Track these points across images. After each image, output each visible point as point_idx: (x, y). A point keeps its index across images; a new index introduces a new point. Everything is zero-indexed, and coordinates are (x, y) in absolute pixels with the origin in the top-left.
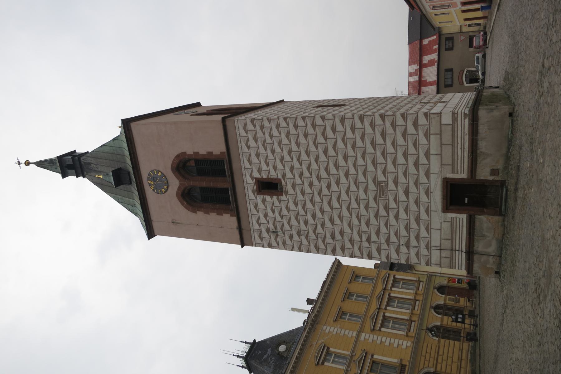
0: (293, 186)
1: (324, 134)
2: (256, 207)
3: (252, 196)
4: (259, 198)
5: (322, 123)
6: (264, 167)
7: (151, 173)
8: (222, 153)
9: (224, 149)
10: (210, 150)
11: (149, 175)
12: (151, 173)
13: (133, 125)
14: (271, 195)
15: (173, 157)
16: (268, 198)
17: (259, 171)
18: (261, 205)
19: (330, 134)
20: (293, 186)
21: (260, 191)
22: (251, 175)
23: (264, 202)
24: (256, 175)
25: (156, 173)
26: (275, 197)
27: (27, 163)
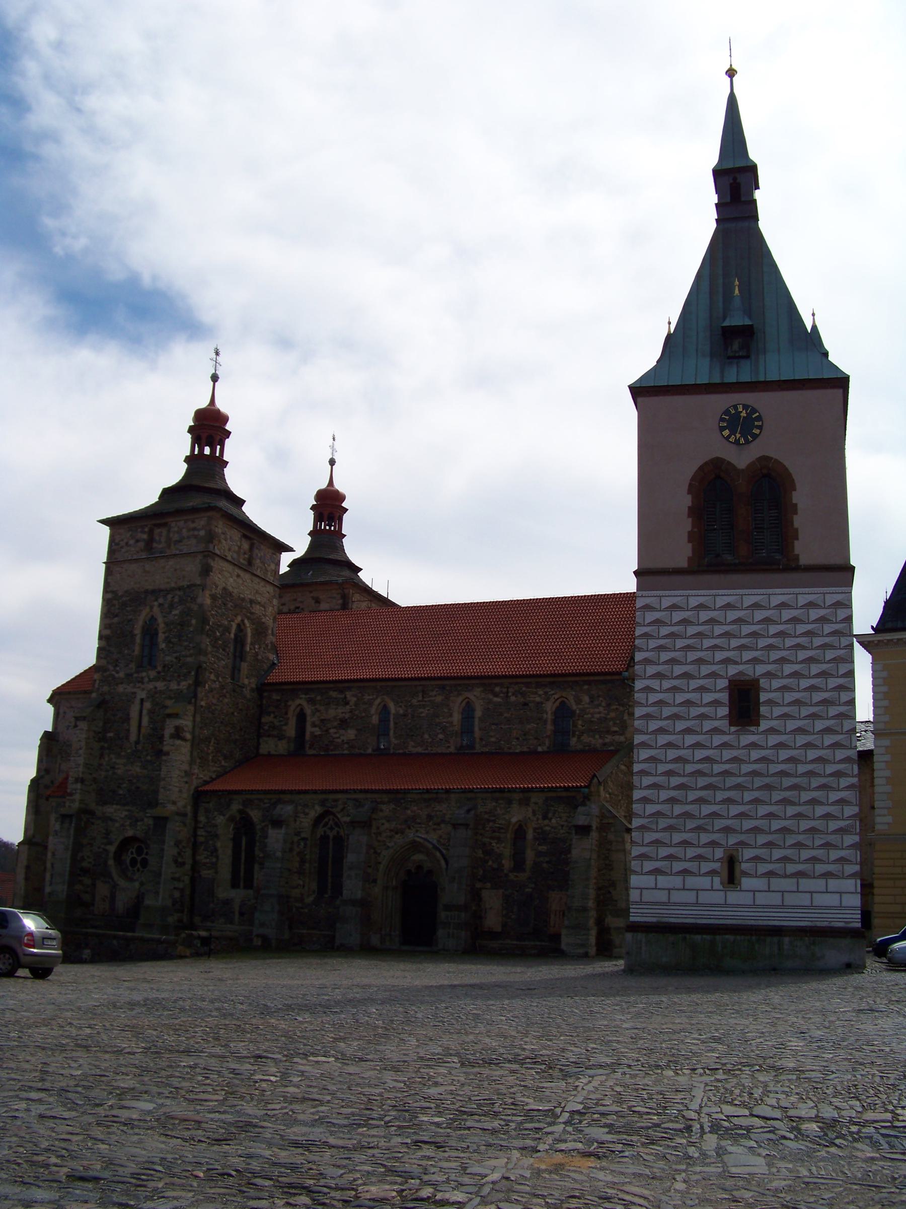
1: (828, 730)
5: (845, 729)
7: (757, 414)
8: (797, 558)
12: (757, 414)
15: (786, 463)
19: (829, 740)
27: (731, 73)
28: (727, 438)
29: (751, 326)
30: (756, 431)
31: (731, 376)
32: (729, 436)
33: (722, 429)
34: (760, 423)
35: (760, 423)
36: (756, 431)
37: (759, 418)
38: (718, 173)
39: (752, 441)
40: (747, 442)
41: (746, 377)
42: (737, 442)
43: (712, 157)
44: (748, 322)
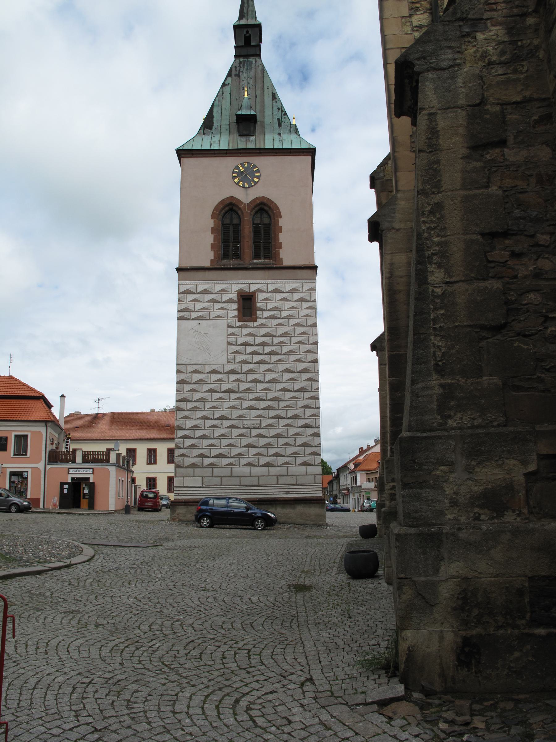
0: (250, 335)
2: (223, 291)
3: (236, 288)
4: (235, 296)
6: (270, 305)
9: (286, 262)
10: (284, 245)
11: (255, 166)
13: (309, 158)
14: (238, 309)
16: (235, 306)
17: (267, 300)
18: (226, 297)
20: (250, 335)
21: (241, 296)
22: (259, 290)
23: (231, 300)
24: (260, 297)
25: (256, 175)
26: (236, 313)
28: (237, 184)
29: (254, 116)
30: (256, 180)
31: (241, 146)
32: (239, 182)
33: (234, 178)
34: (258, 174)
35: (258, 174)
36: (256, 180)
37: (258, 171)
38: (236, 27)
39: (253, 186)
40: (250, 186)
41: (250, 146)
42: (243, 187)
43: (233, 17)
44: (252, 112)
